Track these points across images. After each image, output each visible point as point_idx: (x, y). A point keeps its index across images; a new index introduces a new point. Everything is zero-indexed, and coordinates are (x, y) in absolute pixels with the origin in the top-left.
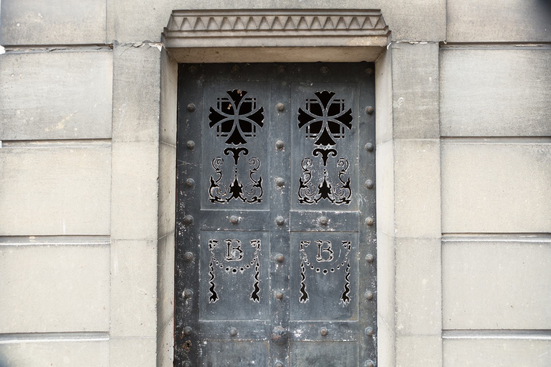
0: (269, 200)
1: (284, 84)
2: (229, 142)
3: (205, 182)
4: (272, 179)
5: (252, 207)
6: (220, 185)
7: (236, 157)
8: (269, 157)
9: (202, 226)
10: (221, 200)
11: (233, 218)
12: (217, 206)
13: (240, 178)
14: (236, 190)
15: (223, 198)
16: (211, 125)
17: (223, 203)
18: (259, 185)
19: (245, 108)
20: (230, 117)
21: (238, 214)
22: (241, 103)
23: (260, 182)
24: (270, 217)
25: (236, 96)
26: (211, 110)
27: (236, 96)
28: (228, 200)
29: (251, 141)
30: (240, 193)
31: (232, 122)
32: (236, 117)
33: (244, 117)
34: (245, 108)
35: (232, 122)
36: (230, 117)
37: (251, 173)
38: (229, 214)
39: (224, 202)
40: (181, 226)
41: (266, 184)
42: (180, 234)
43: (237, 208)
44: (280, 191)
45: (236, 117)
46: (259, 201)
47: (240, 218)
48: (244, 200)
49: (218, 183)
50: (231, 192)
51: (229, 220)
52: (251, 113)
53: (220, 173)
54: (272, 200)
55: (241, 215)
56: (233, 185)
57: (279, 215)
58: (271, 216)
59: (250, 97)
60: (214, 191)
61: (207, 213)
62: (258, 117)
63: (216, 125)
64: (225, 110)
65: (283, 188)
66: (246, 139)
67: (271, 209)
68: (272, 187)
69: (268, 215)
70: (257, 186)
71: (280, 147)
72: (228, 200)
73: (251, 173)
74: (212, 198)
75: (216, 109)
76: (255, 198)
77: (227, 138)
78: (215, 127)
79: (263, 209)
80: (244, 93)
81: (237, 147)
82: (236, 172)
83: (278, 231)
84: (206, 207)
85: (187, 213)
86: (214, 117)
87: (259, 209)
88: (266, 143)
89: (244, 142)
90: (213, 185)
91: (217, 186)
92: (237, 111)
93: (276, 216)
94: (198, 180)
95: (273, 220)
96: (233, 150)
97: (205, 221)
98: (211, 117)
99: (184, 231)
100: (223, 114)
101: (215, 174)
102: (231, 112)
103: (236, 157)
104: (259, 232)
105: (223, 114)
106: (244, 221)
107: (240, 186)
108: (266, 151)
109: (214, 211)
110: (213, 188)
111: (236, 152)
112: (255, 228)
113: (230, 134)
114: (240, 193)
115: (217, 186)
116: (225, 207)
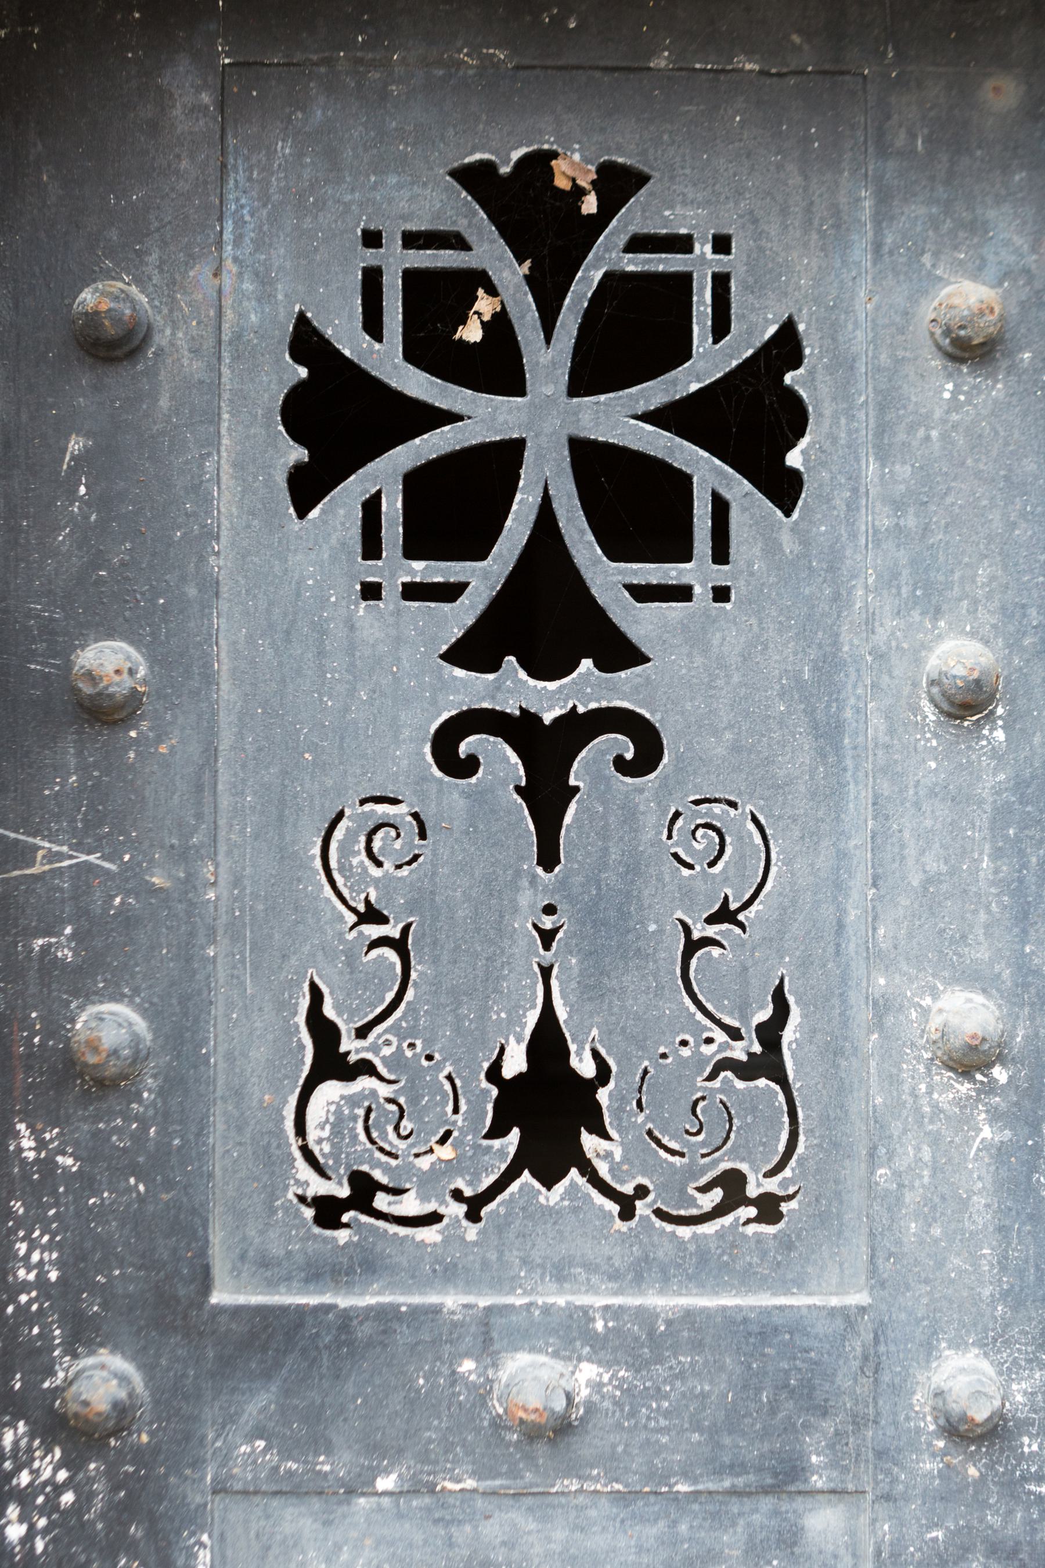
0: (857, 1198)
1: (1002, 94)
2: (474, 652)
3: (256, 1043)
4: (883, 1008)
5: (703, 1267)
6: (396, 1061)
7: (547, 797)
8: (858, 797)
9: (226, 1457)
10: (410, 1205)
11: (532, 1379)
12: (365, 1265)
13: (591, 990)
14: (548, 1110)
15: (428, 1182)
16: (307, 489)
17: (429, 1234)
18: (768, 1063)
19: (637, 329)
20: (482, 418)
21: (571, 1334)
22: (589, 277)
23: (770, 1034)
24: (872, 1363)
25: (538, 216)
26: (307, 343)
27: (538, 216)
28: (475, 1206)
29: (691, 650)
30: (589, 1142)
31: (502, 460)
32: (545, 419)
33: (618, 419)
34: (637, 329)
35: (502, 460)
36: (482, 418)
37: (692, 946)
38: (489, 1335)
39: (434, 1218)
40: (23, 1459)
41: (835, 1050)
42: (15, 1532)
43: (560, 1274)
44: (964, 1122)
45: (545, 419)
46: (769, 1209)
47: (588, 1371)
48: (627, 1213)
49: (379, 1048)
50: (497, 1131)
51: (482, 1394)
52: (687, 380)
53: (400, 945)
54: (893, 1202)
55: (600, 1347)
56: (515, 1064)
57: (959, 1344)
58: (881, 1348)
59: (677, 220)
60: (338, 1125)
61: (271, 1339)
62: (756, 419)
63: (353, 490)
64: (429, 348)
65: (991, 1088)
66: (638, 621)
67: (876, 1281)
68: (893, 1080)
69: (856, 1346)
70: (746, 1070)
71: (967, 704)
72: (475, 1206)
73: (692, 946)
74: (318, 1187)
75: (348, 338)
76: (732, 1184)
77: (459, 618)
78: (341, 507)
79: (800, 1284)
80: (618, 184)
81: (551, 699)
82: (547, 937)
83: (949, 1491)
84: (266, 1268)
85: (83, 1335)
86: (336, 418)
87: (763, 1284)
88: (830, 666)
89: (619, 653)
90: (331, 1064)
91: (366, 1068)
92: (547, 360)
93: (929, 1350)
94: (181, 1024)
95: (901, 1389)
96: (519, 729)
97: (259, 1403)
98: (299, 413)
99: (51, 1506)
100: (417, 384)
101: (351, 961)
102: (497, 367)
103: (547, 797)
104: (767, 1503)
105: (417, 384)
106: (631, 1399)
107: (587, 1069)
108: (829, 735)
109: (346, 1317)
110: (330, 1091)
111: (547, 751)
112: (737, 1467)
113: (484, 578)
114: (589, 1142)
115: (366, 1068)
116: (448, 1273)
